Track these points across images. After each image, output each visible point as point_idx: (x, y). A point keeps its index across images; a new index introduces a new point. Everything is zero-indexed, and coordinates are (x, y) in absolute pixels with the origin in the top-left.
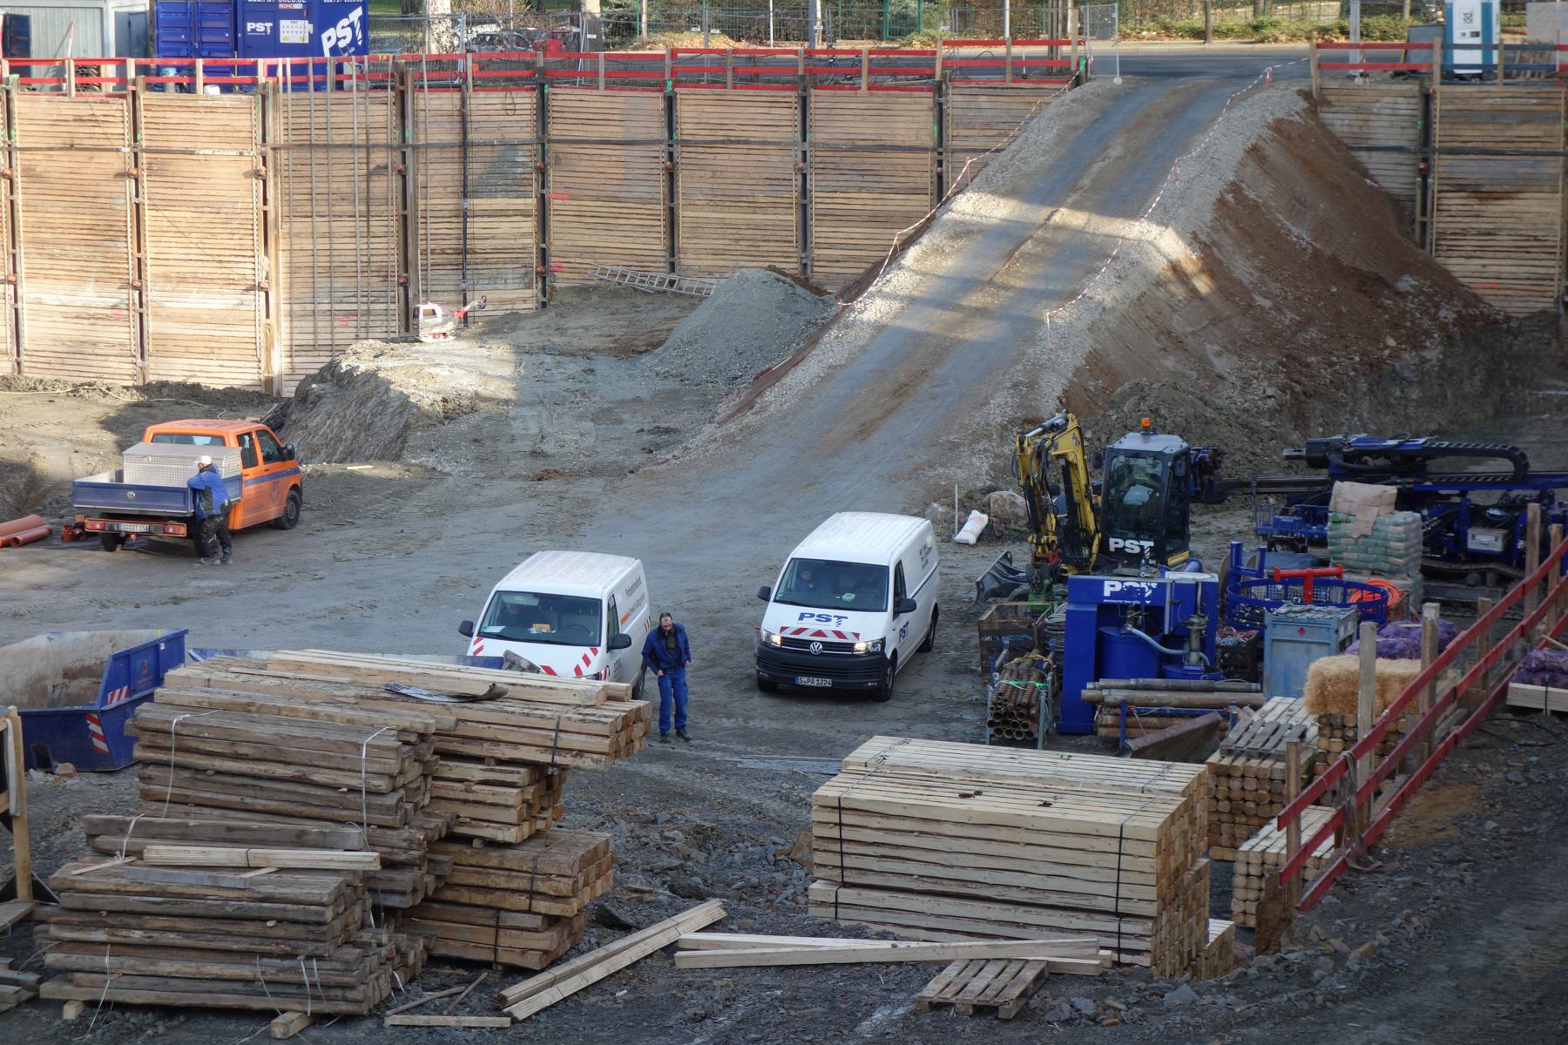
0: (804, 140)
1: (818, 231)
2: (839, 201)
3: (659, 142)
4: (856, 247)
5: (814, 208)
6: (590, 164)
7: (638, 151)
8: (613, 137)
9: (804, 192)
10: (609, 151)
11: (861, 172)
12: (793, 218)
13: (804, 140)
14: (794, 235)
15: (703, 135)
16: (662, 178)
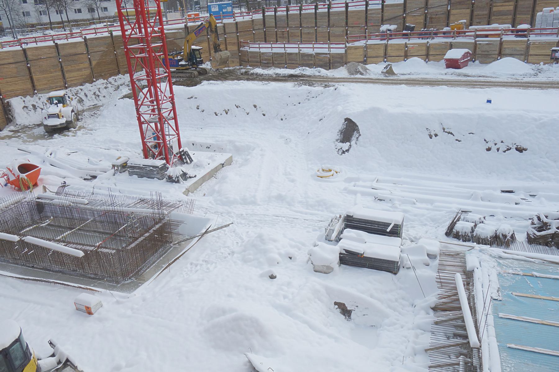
0: (59, 55)
1: (67, 75)
2: (69, 68)
3: (23, 62)
4: (75, 77)
5: (65, 70)
6: (7, 69)
7: (19, 64)
8: (11, 62)
9: (62, 67)
10: (11, 66)
11: (73, 61)
12: (60, 73)
13: (59, 55)
14: (61, 77)
15: (35, 58)
16: (27, 70)
